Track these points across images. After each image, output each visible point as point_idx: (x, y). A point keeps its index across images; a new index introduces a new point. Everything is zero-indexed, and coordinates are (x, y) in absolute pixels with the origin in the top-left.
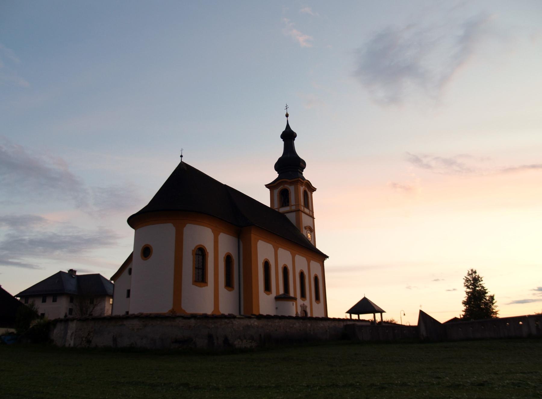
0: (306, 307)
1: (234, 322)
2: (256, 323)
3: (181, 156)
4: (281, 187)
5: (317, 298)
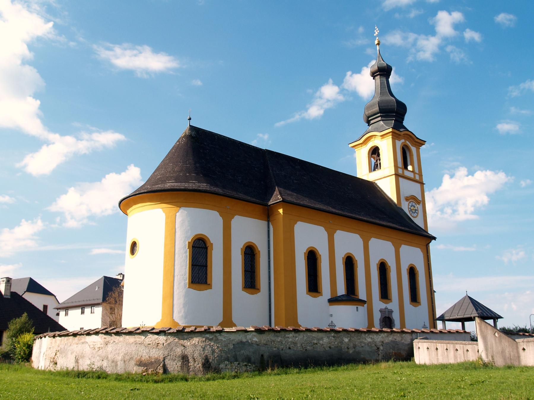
0: (391, 312)
1: (220, 338)
2: (255, 339)
3: (190, 119)
5: (414, 298)
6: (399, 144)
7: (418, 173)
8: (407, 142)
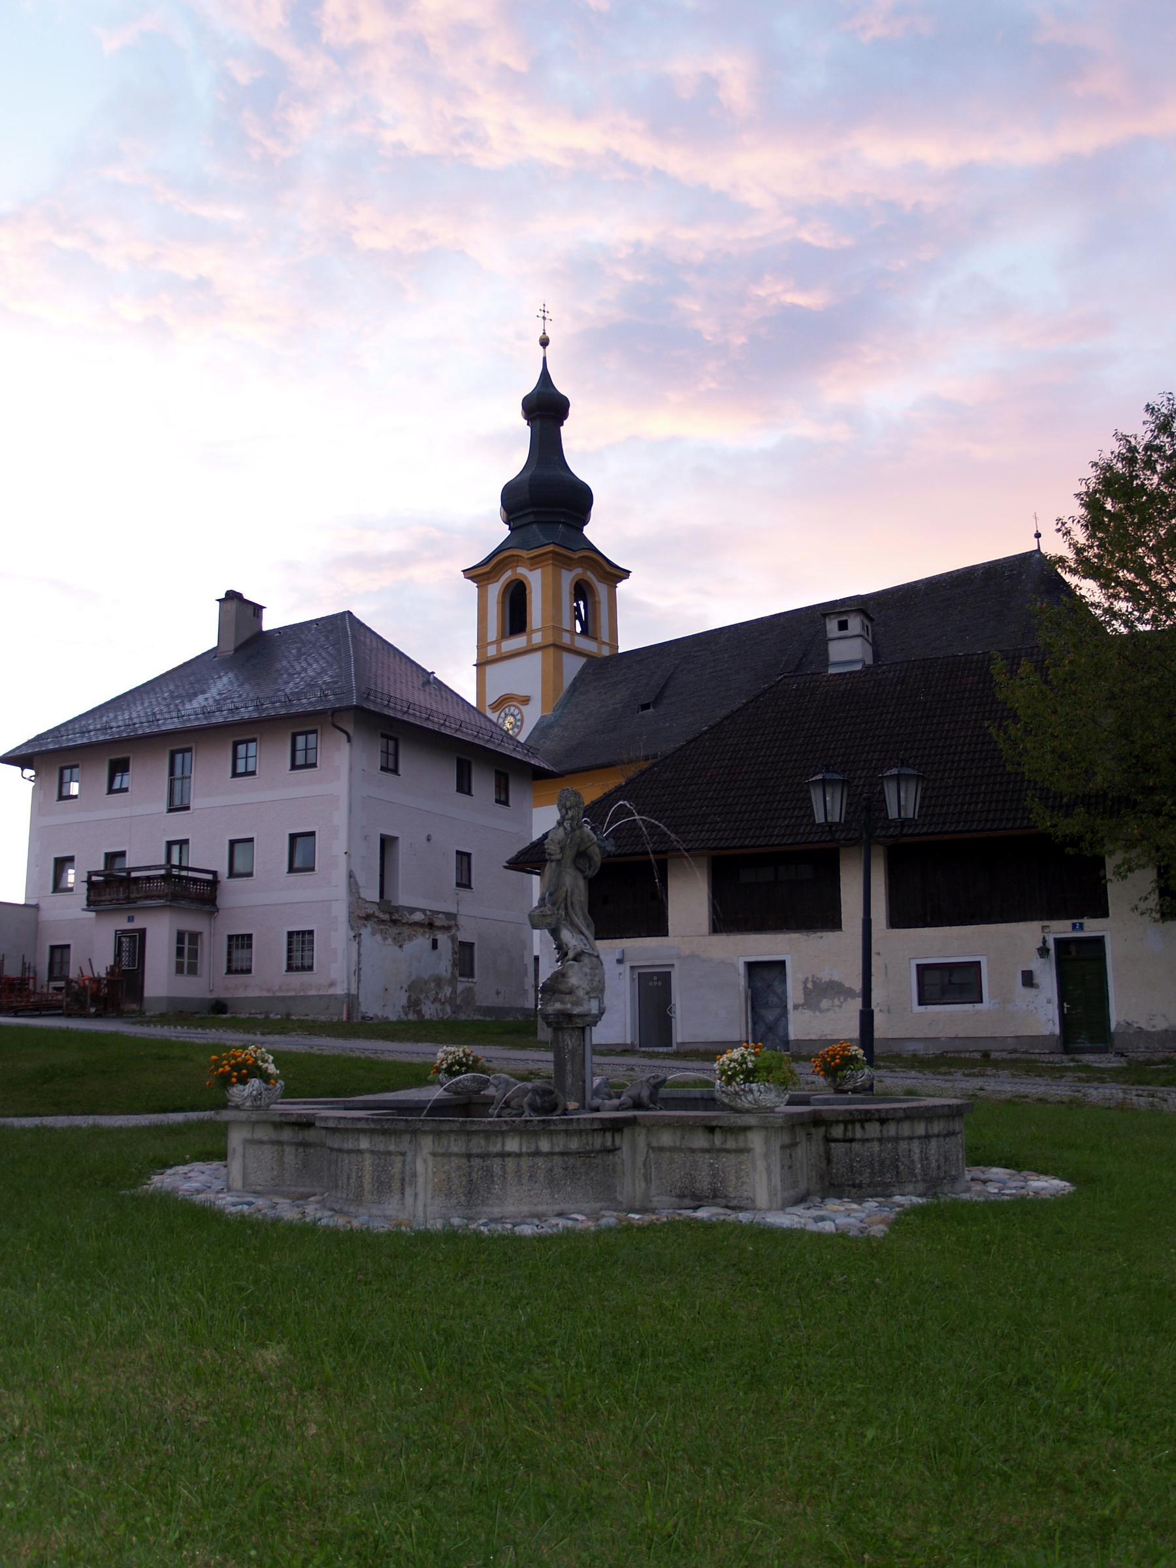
4: (507, 576)
6: (568, 578)
7: (607, 641)
8: (589, 574)
